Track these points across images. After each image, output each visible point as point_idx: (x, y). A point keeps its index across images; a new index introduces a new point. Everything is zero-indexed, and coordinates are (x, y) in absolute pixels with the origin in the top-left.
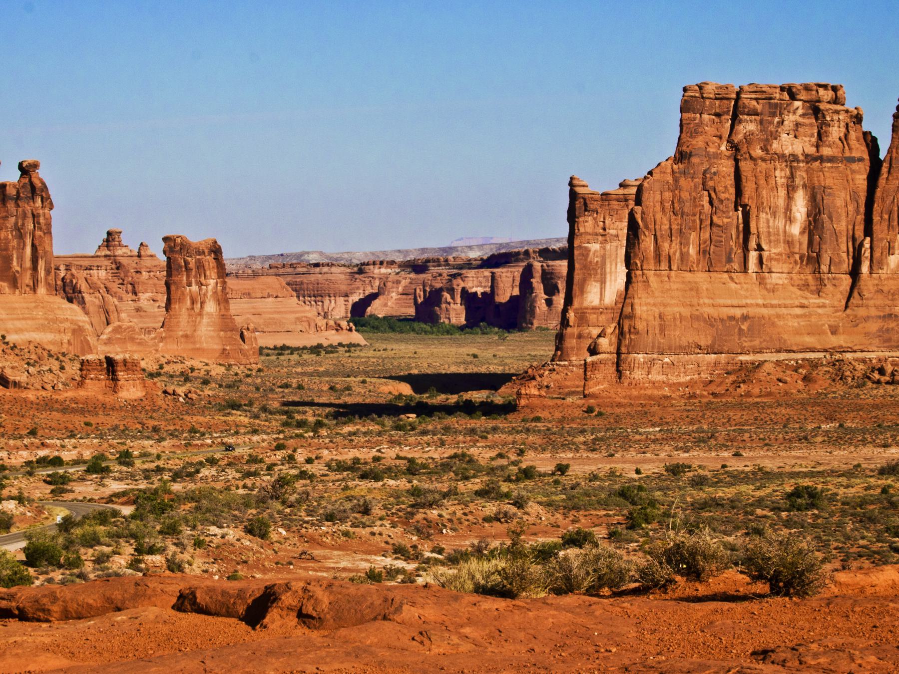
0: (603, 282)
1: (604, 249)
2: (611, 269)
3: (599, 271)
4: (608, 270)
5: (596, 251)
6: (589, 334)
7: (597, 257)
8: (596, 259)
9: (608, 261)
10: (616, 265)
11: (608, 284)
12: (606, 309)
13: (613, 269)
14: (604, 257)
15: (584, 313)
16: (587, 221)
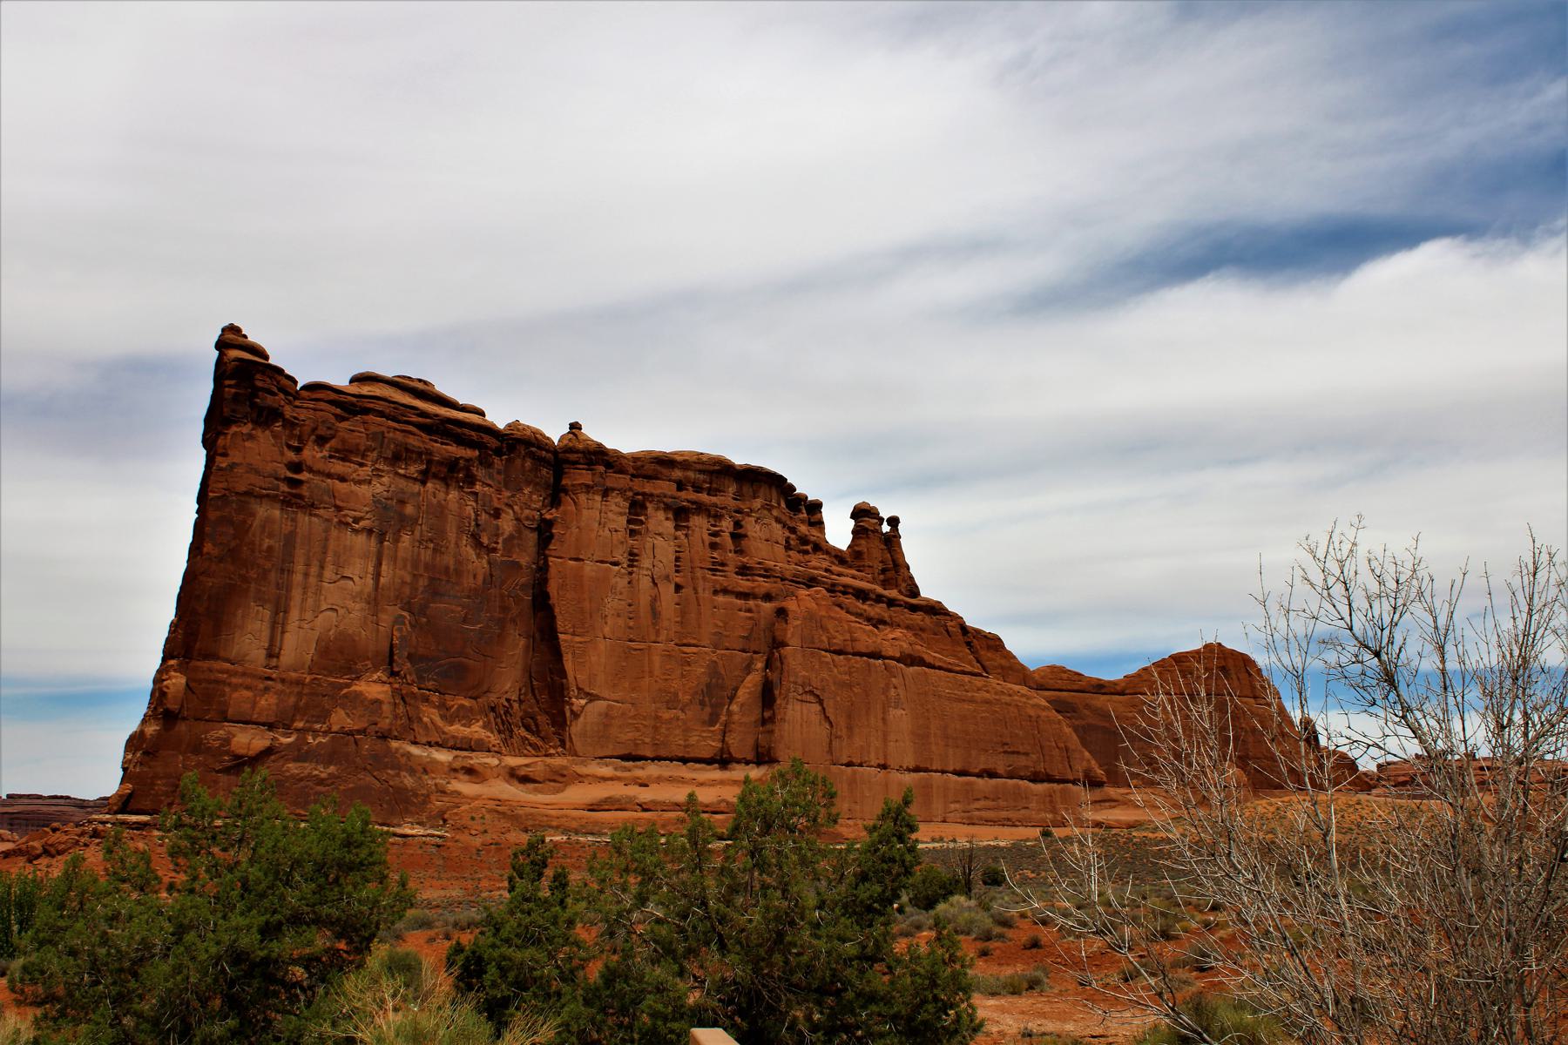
0: (280, 610)
1: (293, 520)
2: (306, 575)
3: (273, 576)
4: (298, 578)
5: (268, 521)
6: (227, 741)
7: (271, 536)
8: (267, 542)
9: (300, 555)
10: (322, 567)
11: (294, 614)
12: (283, 681)
13: (312, 580)
14: (290, 540)
15: (217, 682)
16: (251, 437)
